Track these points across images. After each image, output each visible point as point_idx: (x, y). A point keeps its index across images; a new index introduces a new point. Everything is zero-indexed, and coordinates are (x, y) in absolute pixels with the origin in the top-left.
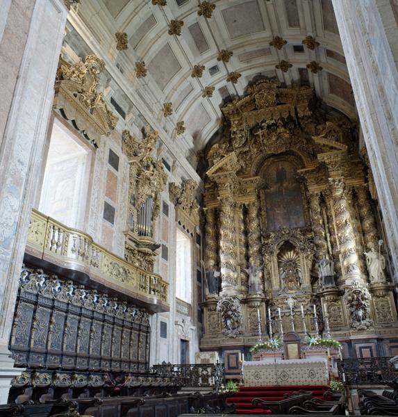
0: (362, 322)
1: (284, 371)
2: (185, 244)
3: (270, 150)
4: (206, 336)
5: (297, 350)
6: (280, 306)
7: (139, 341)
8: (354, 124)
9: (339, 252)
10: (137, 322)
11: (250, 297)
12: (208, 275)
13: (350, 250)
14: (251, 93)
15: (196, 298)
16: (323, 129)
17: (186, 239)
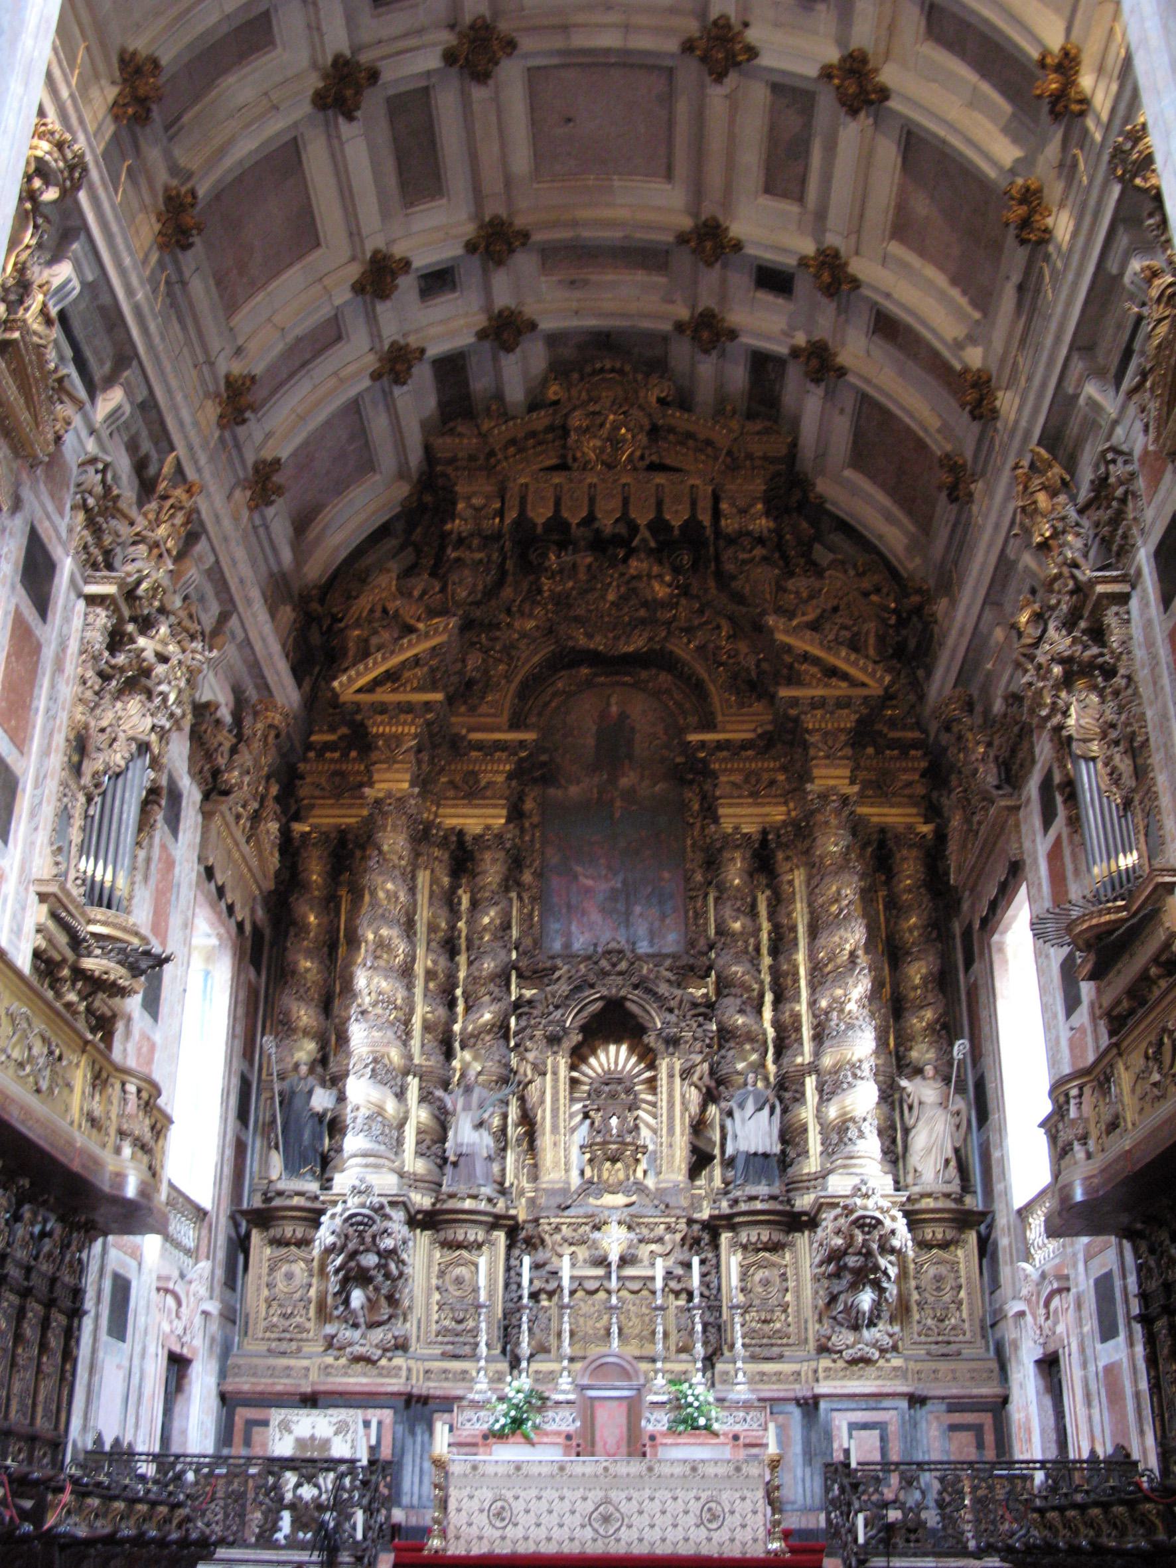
0: (865, 1332)
1: (607, 1501)
2: (209, 959)
3: (590, 636)
4: (251, 1346)
6: (567, 1250)
7: (43, 1347)
8: (915, 599)
9: (814, 1068)
10: (44, 1267)
12: (287, 1100)
13: (855, 1067)
14: (556, 403)
15: (226, 1184)
16: (811, 597)
17: (214, 941)
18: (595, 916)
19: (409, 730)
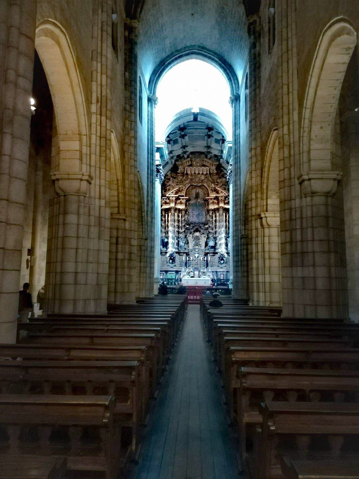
5: (198, 274)
13: (222, 238)
18: (195, 217)
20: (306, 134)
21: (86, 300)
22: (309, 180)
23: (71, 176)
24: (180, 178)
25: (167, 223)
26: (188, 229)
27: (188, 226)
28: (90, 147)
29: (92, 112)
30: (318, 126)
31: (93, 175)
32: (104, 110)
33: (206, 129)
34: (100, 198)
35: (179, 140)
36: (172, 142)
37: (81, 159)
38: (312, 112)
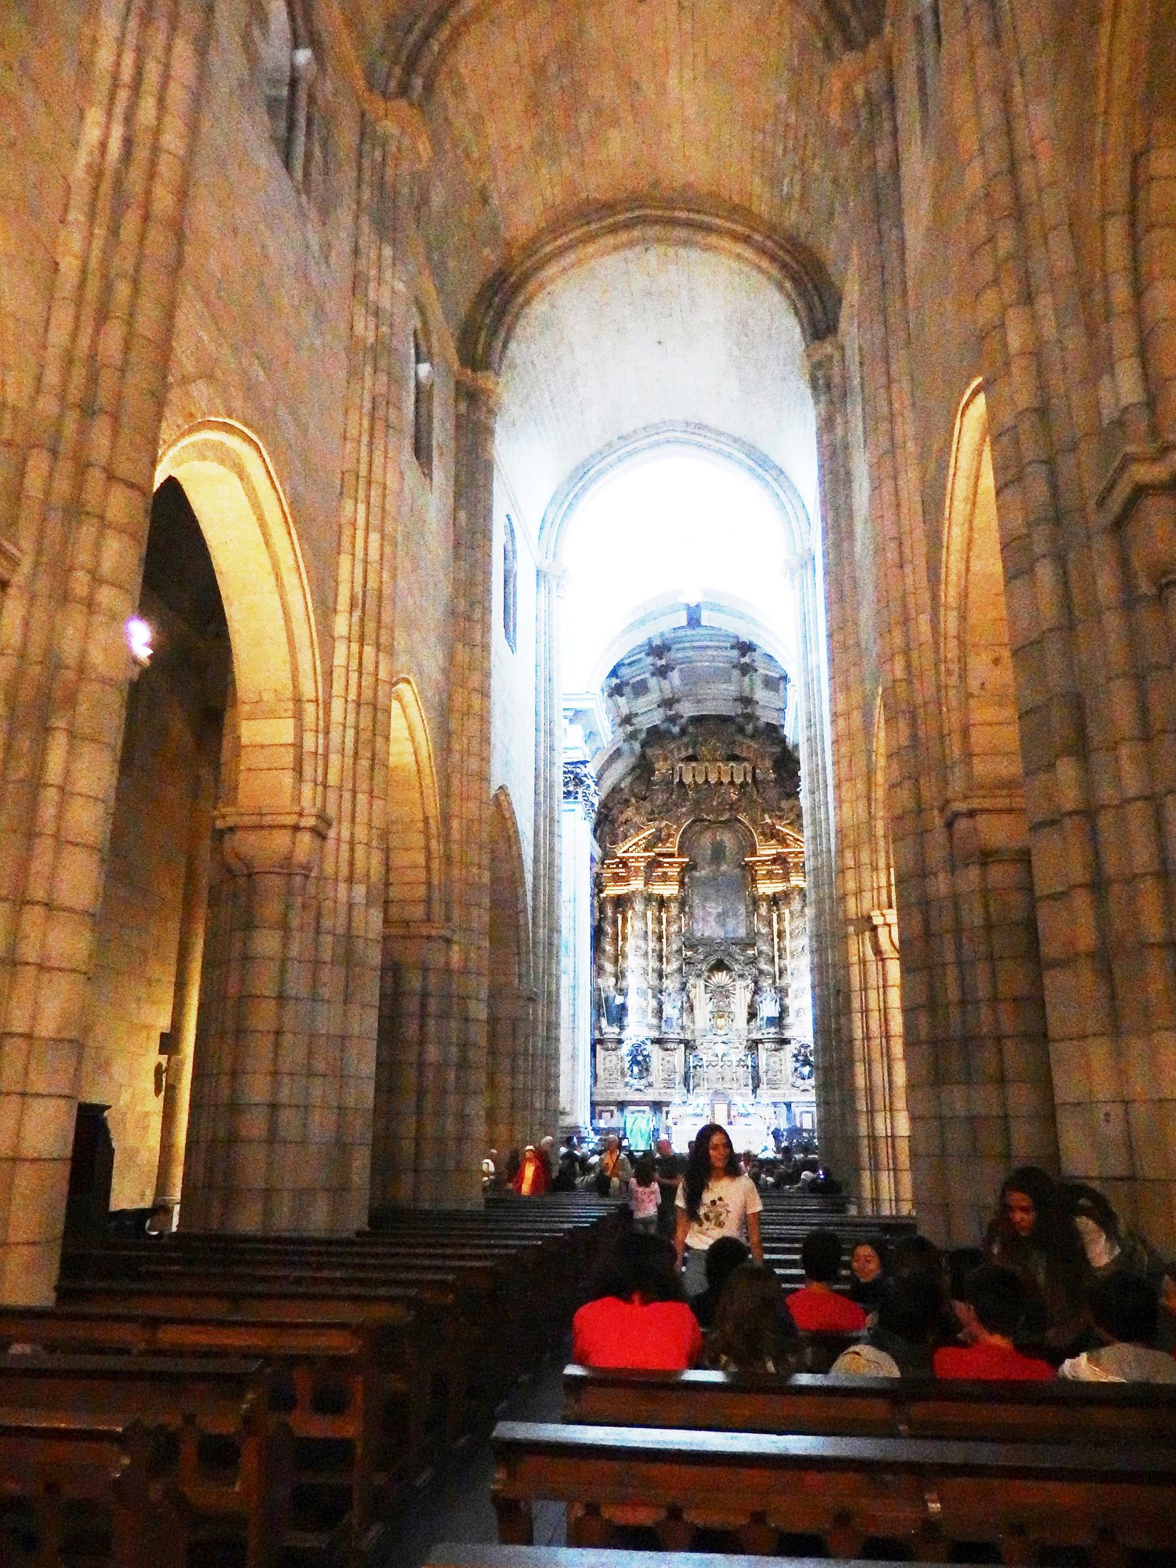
11: (666, 1036)
12: (607, 999)
18: (713, 924)
19: (642, 865)
20: (953, 680)
21: (303, 1195)
22: (971, 814)
23: (268, 820)
24: (660, 798)
25: (620, 943)
26: (689, 963)
27: (689, 953)
28: (327, 733)
29: (336, 635)
30: (986, 657)
31: (332, 812)
32: (371, 626)
33: (733, 647)
34: (350, 880)
35: (653, 682)
36: (627, 690)
37: (298, 770)
38: (963, 618)
